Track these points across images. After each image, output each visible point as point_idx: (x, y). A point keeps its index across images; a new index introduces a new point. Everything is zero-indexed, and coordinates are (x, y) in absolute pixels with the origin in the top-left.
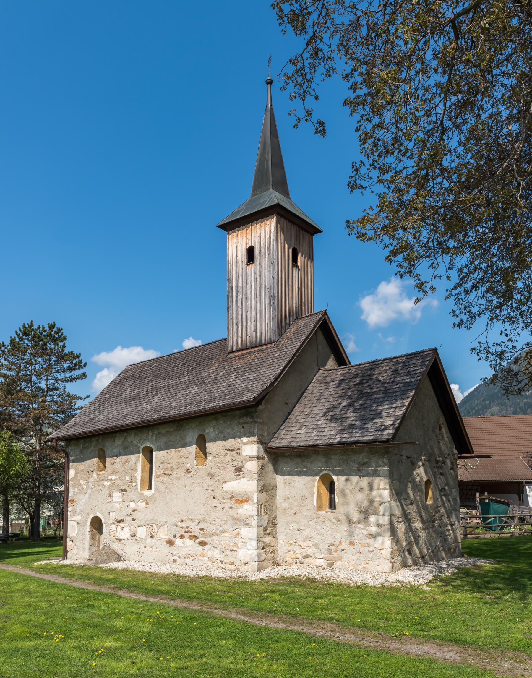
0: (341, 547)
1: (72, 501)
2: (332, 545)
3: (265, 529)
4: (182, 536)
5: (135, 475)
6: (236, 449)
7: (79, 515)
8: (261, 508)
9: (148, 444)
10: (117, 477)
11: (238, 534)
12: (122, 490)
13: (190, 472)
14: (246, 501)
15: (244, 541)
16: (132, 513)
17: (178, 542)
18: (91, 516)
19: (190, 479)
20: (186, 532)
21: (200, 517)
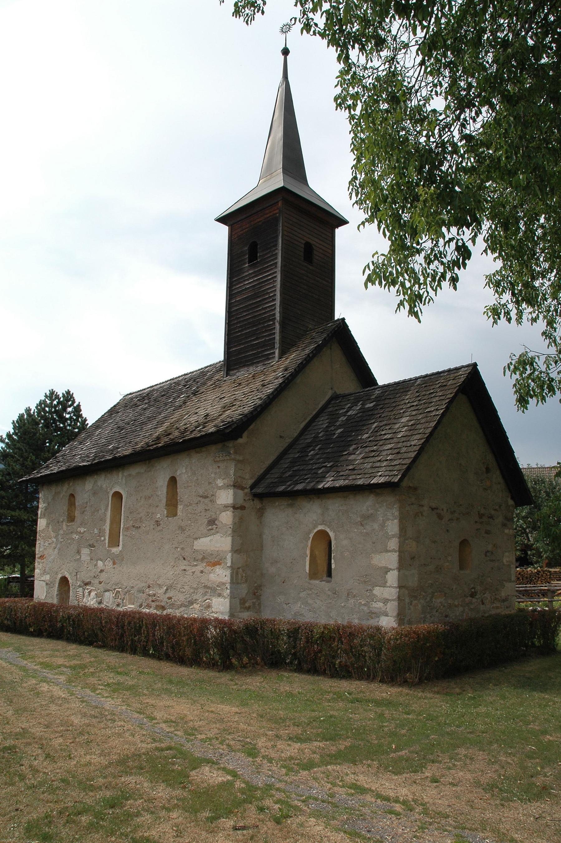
3: (243, 601)
8: (237, 574)
9: (117, 489)
16: (99, 574)
18: (60, 576)
20: (153, 601)
21: (168, 582)
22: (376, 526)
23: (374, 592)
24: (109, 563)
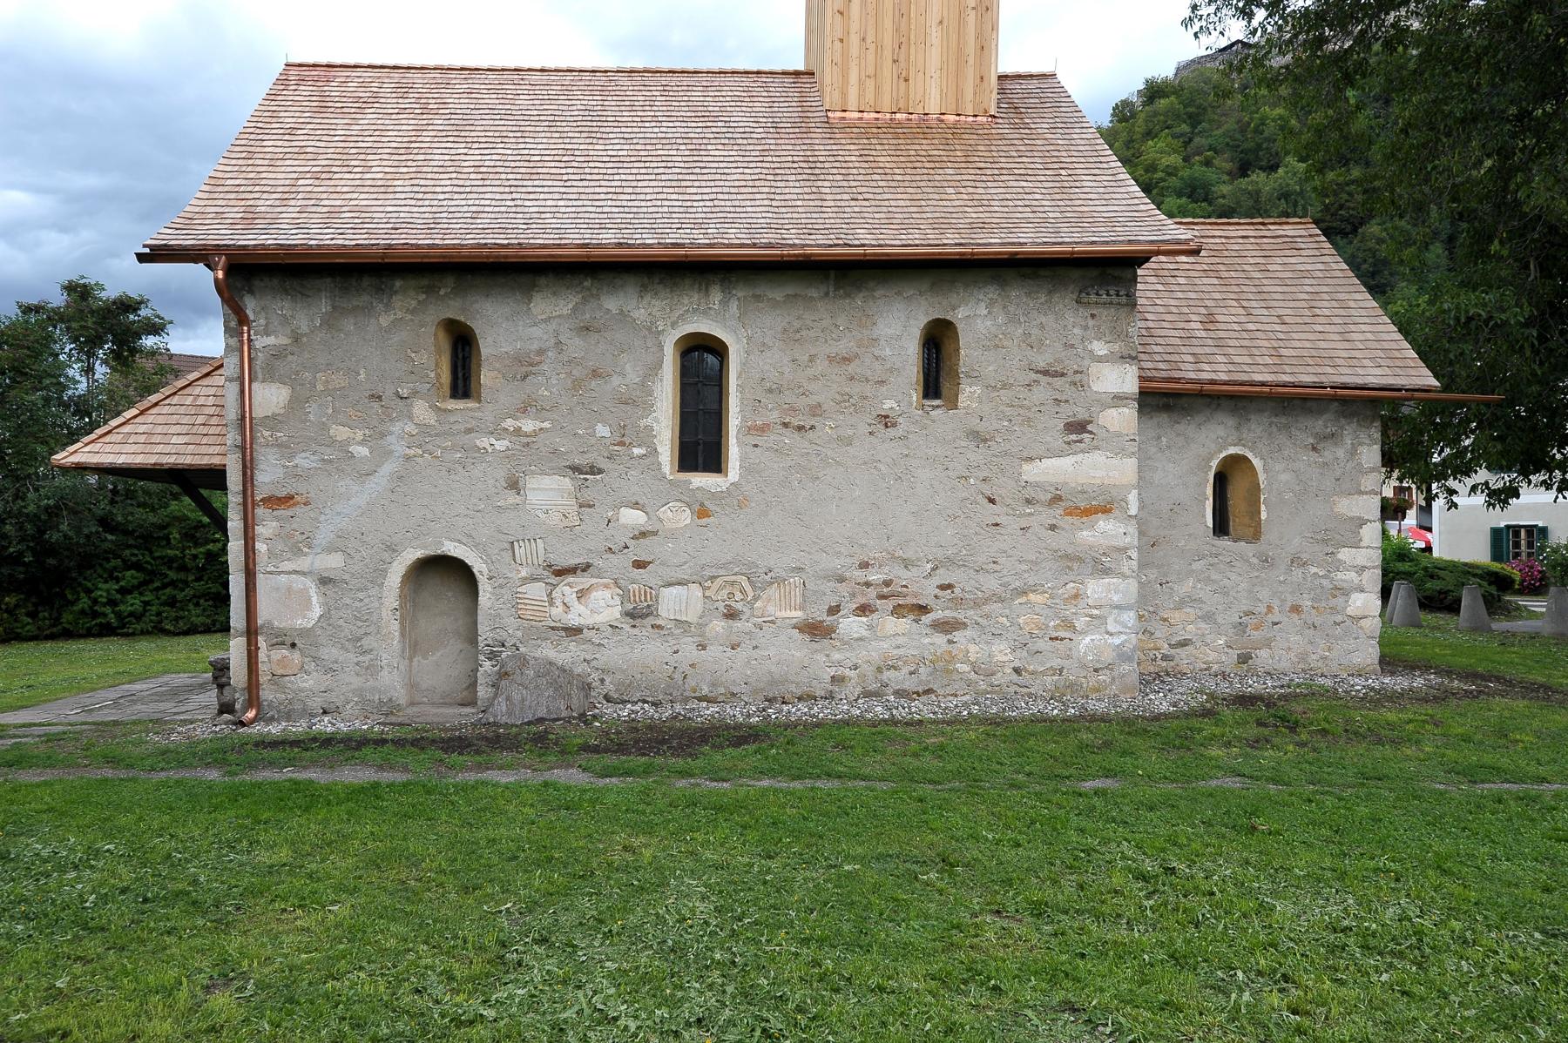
0: (1271, 618)
2: (1248, 613)
4: (864, 610)
5: (643, 423)
6: (1070, 373)
7: (330, 549)
10: (546, 425)
11: (1076, 596)
12: (576, 469)
13: (894, 425)
14: (1106, 510)
15: (1095, 612)
16: (631, 543)
17: (851, 625)
19: (893, 444)
20: (882, 597)
21: (940, 554)
22: (1340, 453)
23: (1340, 556)
24: (678, 517)
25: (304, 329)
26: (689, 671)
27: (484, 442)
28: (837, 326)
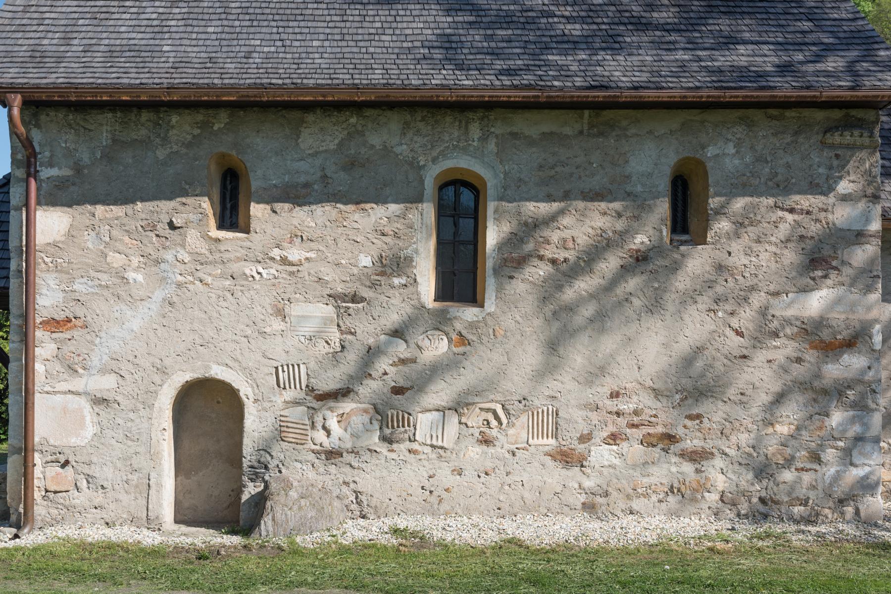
1: (54, 325)
4: (614, 438)
6: (815, 210)
7: (104, 371)
17: (602, 455)
20: (634, 426)
25: (86, 158)
26: (445, 495)
27: (250, 269)
28: (591, 163)
